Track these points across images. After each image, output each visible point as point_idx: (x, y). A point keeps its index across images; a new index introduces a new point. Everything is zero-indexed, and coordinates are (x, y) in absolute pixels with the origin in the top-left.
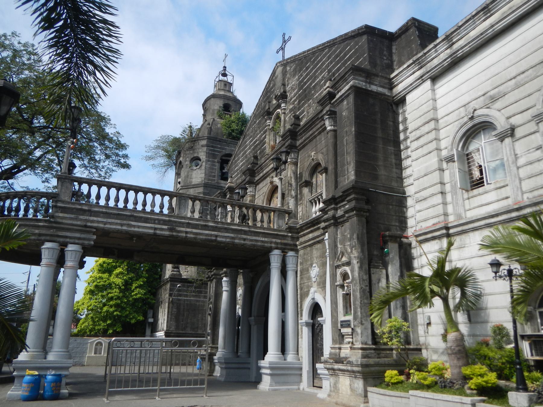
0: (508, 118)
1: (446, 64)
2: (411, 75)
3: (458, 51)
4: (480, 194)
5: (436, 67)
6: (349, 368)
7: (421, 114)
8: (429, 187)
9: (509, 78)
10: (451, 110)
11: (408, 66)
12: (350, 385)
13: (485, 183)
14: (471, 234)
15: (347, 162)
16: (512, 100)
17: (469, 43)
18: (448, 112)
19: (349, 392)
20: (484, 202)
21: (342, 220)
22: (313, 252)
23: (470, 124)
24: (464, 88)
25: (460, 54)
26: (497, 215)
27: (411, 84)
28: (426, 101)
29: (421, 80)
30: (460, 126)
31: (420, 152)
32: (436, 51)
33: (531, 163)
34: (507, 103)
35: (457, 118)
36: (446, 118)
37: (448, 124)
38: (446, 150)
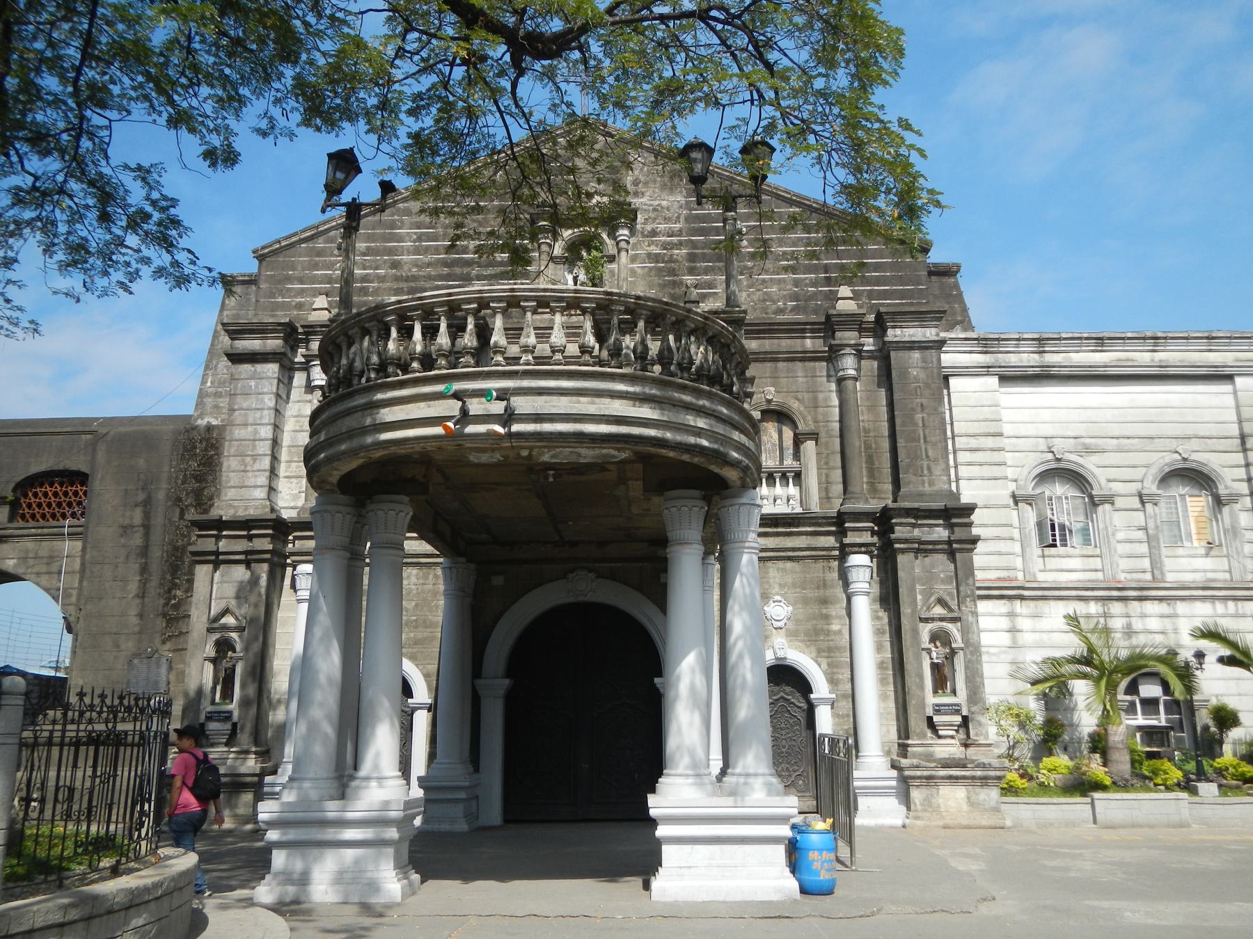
0: (1109, 481)
1: (1031, 371)
2: (965, 352)
3: (1054, 367)
4: (1059, 556)
5: (1015, 367)
6: (979, 773)
7: (981, 418)
8: (993, 526)
9: (1111, 435)
10: (1023, 433)
11: (966, 339)
12: (969, 798)
13: (1058, 543)
14: (1052, 603)
15: (927, 456)
16: (1113, 462)
17: (1071, 367)
18: (1017, 434)
19: (965, 807)
20: (1064, 567)
21: (930, 547)
22: (767, 573)
23: (1054, 465)
24: (1046, 415)
25: (1054, 371)
26: (1093, 589)
27: (967, 367)
28: (989, 403)
29: (986, 370)
30: (1040, 461)
31: (975, 471)
32: (1017, 346)
33: (1131, 542)
34: (1107, 463)
35: (1034, 449)
36: (1014, 440)
37: (1018, 449)
38: (1014, 484)
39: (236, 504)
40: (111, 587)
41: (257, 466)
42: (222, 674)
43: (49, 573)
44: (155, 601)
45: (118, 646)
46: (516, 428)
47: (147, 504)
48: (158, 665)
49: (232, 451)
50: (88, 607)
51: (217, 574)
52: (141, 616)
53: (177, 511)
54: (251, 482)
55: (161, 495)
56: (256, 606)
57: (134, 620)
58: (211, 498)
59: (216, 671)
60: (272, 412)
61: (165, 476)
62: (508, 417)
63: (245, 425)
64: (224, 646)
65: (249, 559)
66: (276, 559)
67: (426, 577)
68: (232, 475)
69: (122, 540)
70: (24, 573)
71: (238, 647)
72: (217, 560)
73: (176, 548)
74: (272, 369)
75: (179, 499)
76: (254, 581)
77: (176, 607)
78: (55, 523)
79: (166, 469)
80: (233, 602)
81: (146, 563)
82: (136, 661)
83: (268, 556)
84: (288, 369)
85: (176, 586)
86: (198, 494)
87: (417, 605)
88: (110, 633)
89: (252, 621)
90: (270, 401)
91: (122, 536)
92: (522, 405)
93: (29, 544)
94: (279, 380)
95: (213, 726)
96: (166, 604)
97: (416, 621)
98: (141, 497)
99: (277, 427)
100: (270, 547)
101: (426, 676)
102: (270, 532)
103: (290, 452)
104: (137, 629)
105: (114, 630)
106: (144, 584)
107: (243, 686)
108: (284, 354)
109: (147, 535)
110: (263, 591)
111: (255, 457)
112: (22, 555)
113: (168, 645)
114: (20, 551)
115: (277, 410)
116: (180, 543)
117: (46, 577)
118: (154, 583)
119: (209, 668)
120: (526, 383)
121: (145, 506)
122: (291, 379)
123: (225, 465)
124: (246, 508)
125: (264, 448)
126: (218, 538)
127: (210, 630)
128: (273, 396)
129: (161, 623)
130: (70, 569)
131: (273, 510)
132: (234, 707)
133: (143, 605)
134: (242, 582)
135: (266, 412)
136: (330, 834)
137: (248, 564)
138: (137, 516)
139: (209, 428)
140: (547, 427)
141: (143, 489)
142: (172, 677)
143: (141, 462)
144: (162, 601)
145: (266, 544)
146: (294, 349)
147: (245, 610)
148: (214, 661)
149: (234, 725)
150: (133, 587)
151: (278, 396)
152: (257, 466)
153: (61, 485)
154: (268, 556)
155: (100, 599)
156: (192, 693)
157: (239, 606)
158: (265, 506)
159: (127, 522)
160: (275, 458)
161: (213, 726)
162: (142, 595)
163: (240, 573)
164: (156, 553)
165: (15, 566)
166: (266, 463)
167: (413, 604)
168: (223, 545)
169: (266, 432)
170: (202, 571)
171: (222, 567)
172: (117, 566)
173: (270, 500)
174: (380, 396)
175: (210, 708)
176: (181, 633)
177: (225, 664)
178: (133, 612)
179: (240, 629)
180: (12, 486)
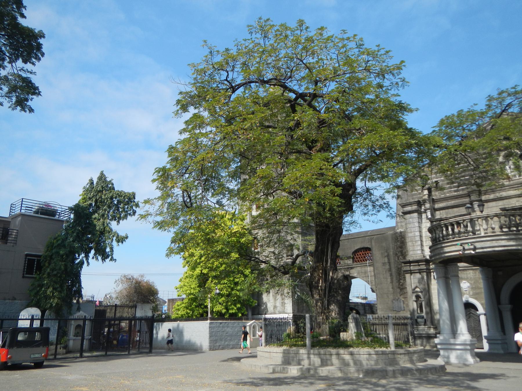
39: (413, 256)
41: (417, 244)
42: (419, 305)
43: (366, 277)
44: (396, 284)
45: (388, 297)
46: (477, 251)
47: (388, 256)
48: (400, 302)
49: (409, 240)
50: (379, 286)
51: (412, 276)
52: (393, 288)
53: (397, 258)
54: (416, 249)
55: (391, 253)
56: (424, 285)
57: (391, 290)
58: (405, 253)
59: (417, 304)
60: (418, 228)
61: (391, 247)
62: (475, 249)
63: (411, 232)
64: (418, 297)
65: (420, 271)
66: (428, 271)
67: (475, 273)
68: (410, 247)
69: (384, 267)
71: (422, 297)
72: (411, 272)
73: (399, 268)
74: (415, 215)
75: (397, 254)
76: (423, 278)
77: (402, 285)
78: (364, 262)
79: (391, 245)
80: (418, 285)
82: (394, 301)
83: (425, 270)
84: (420, 213)
85: (400, 279)
86: (401, 252)
87: (474, 282)
89: (424, 289)
90: (417, 224)
92: (478, 245)
93: (359, 269)
94: (418, 218)
95: (419, 320)
96: (399, 284)
97: (475, 287)
98: (386, 254)
99: (420, 232)
100: (425, 268)
101: (482, 304)
102: (424, 263)
103: (426, 238)
104: (392, 292)
106: (392, 279)
107: (426, 308)
108: (418, 210)
109: (390, 265)
110: (426, 281)
111: (416, 241)
113: (402, 297)
115: (420, 227)
116: (399, 267)
118: (394, 279)
119: (415, 304)
120: (478, 240)
122: (421, 216)
123: (408, 244)
124: (416, 257)
125: (418, 238)
126: (410, 266)
127: (413, 293)
128: (417, 223)
129: (399, 290)
131: (424, 256)
132: (424, 314)
133: (393, 285)
134: (419, 278)
135: (416, 228)
136: (453, 347)
137: (420, 273)
138: (386, 260)
139: (401, 232)
140: (485, 250)
142: (405, 306)
143: (384, 244)
144: (398, 284)
145: (424, 267)
146: (421, 207)
147: (422, 286)
148: (416, 301)
149: (425, 320)
150: (389, 280)
151: (419, 222)
152: (417, 244)
153: (364, 251)
154: (425, 270)
155: (381, 284)
156: (412, 311)
157: (420, 285)
158: (421, 256)
159: (384, 262)
160: (421, 241)
161: (419, 320)
162: (392, 282)
163: (418, 276)
164: (394, 270)
166: (419, 243)
167: (473, 282)
168: (412, 268)
169: (418, 234)
170: (408, 276)
171: (413, 274)
173: (422, 253)
174: (443, 245)
175: (417, 315)
176: (405, 293)
177: (419, 302)
178: (390, 287)
179: (421, 292)
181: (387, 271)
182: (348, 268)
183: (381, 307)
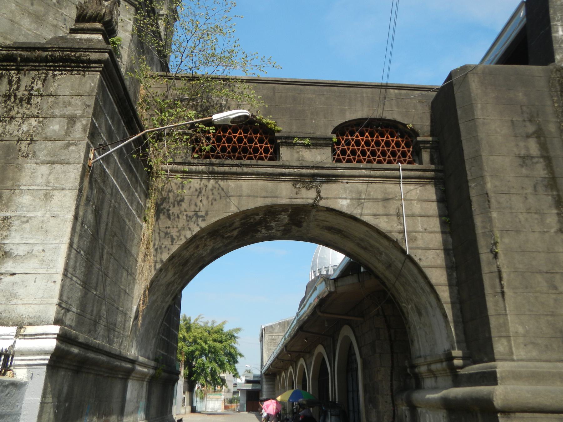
40: (527, 219)
43: (387, 215)
45: (555, 288)
47: (539, 134)
50: (506, 240)
61: (549, 110)
69: (524, 171)
70: (361, 215)
79: (549, 103)
81: (559, 195)
88: (540, 272)
91: (522, 166)
93: (360, 186)
98: (531, 128)
105: (544, 269)
112: (354, 196)
114: (351, 191)
117: (385, 218)
121: (538, 137)
130: (410, 213)
138: (533, 147)
141: (530, 121)
143: (520, 96)
155: (518, 232)
159: (523, 152)
165: (348, 206)
172: (526, 198)
180: (331, 129)
181: (541, 189)
182: (314, 176)
183: (521, 330)
